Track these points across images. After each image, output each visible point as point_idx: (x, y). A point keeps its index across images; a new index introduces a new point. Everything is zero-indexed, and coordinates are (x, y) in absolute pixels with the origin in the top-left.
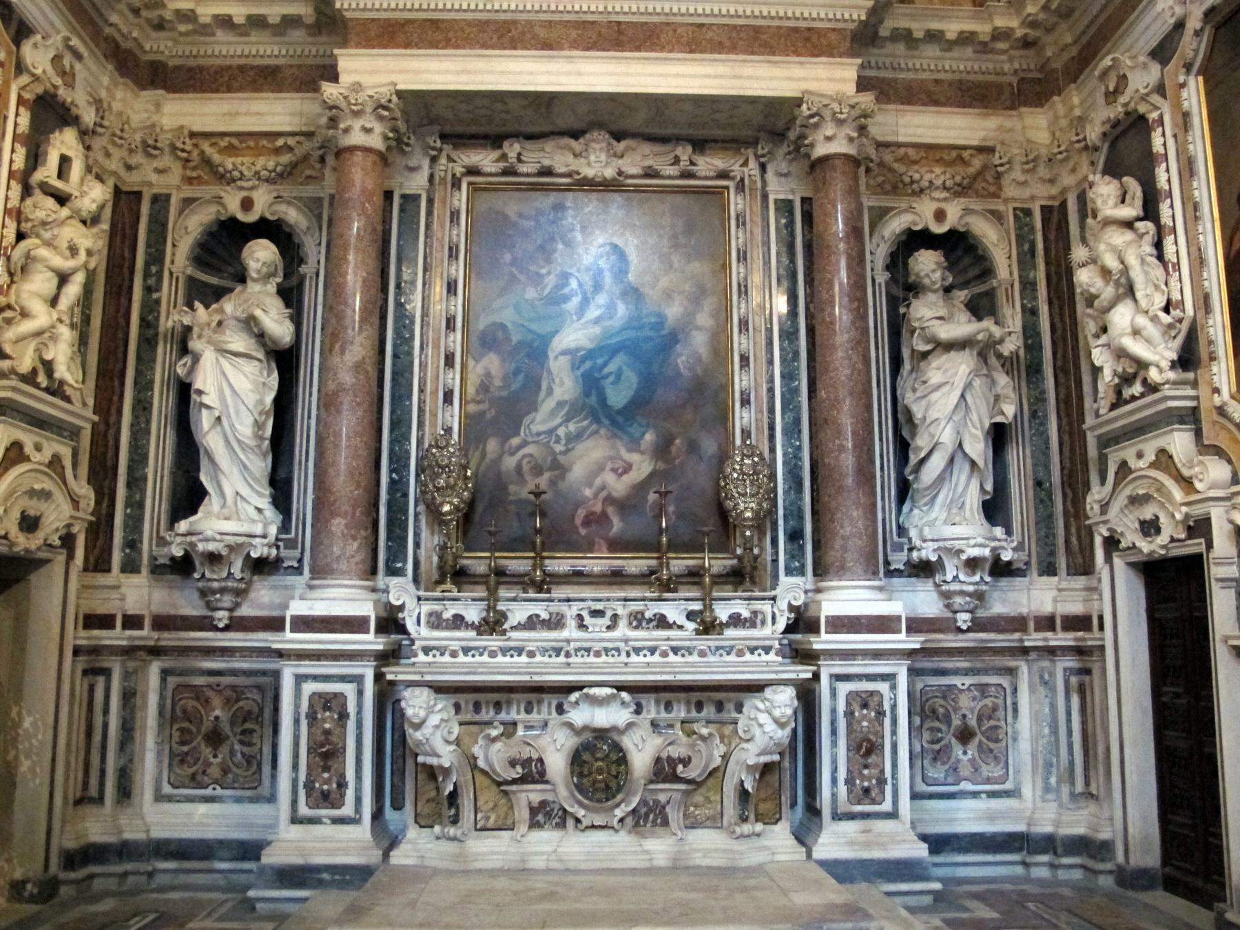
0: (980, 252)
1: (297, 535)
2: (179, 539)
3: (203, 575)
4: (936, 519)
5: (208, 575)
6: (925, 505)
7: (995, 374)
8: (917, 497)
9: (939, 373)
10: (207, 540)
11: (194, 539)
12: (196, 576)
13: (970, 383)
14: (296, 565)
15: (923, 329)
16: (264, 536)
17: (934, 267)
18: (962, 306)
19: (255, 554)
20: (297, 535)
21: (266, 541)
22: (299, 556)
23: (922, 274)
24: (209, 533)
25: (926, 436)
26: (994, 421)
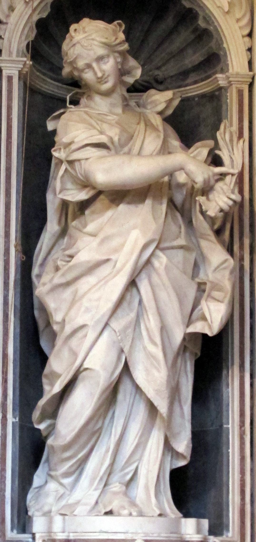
0: (201, 23)
4: (78, 503)
6: (67, 475)
7: (204, 243)
8: (54, 459)
9: (94, 242)
13: (148, 262)
15: (71, 163)
17: (101, 51)
18: (157, 121)
23: (81, 64)
25: (66, 353)
26: (191, 329)
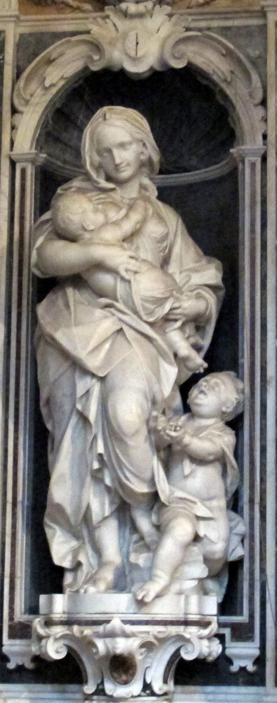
1: (252, 616)
2: (59, 630)
3: (100, 691)
5: (109, 687)
10: (112, 635)
11: (88, 631)
12: (89, 688)
14: (251, 668)
16: (204, 624)
19: (188, 656)
20: (252, 616)
21: (205, 632)
22: (256, 652)
24: (116, 623)
